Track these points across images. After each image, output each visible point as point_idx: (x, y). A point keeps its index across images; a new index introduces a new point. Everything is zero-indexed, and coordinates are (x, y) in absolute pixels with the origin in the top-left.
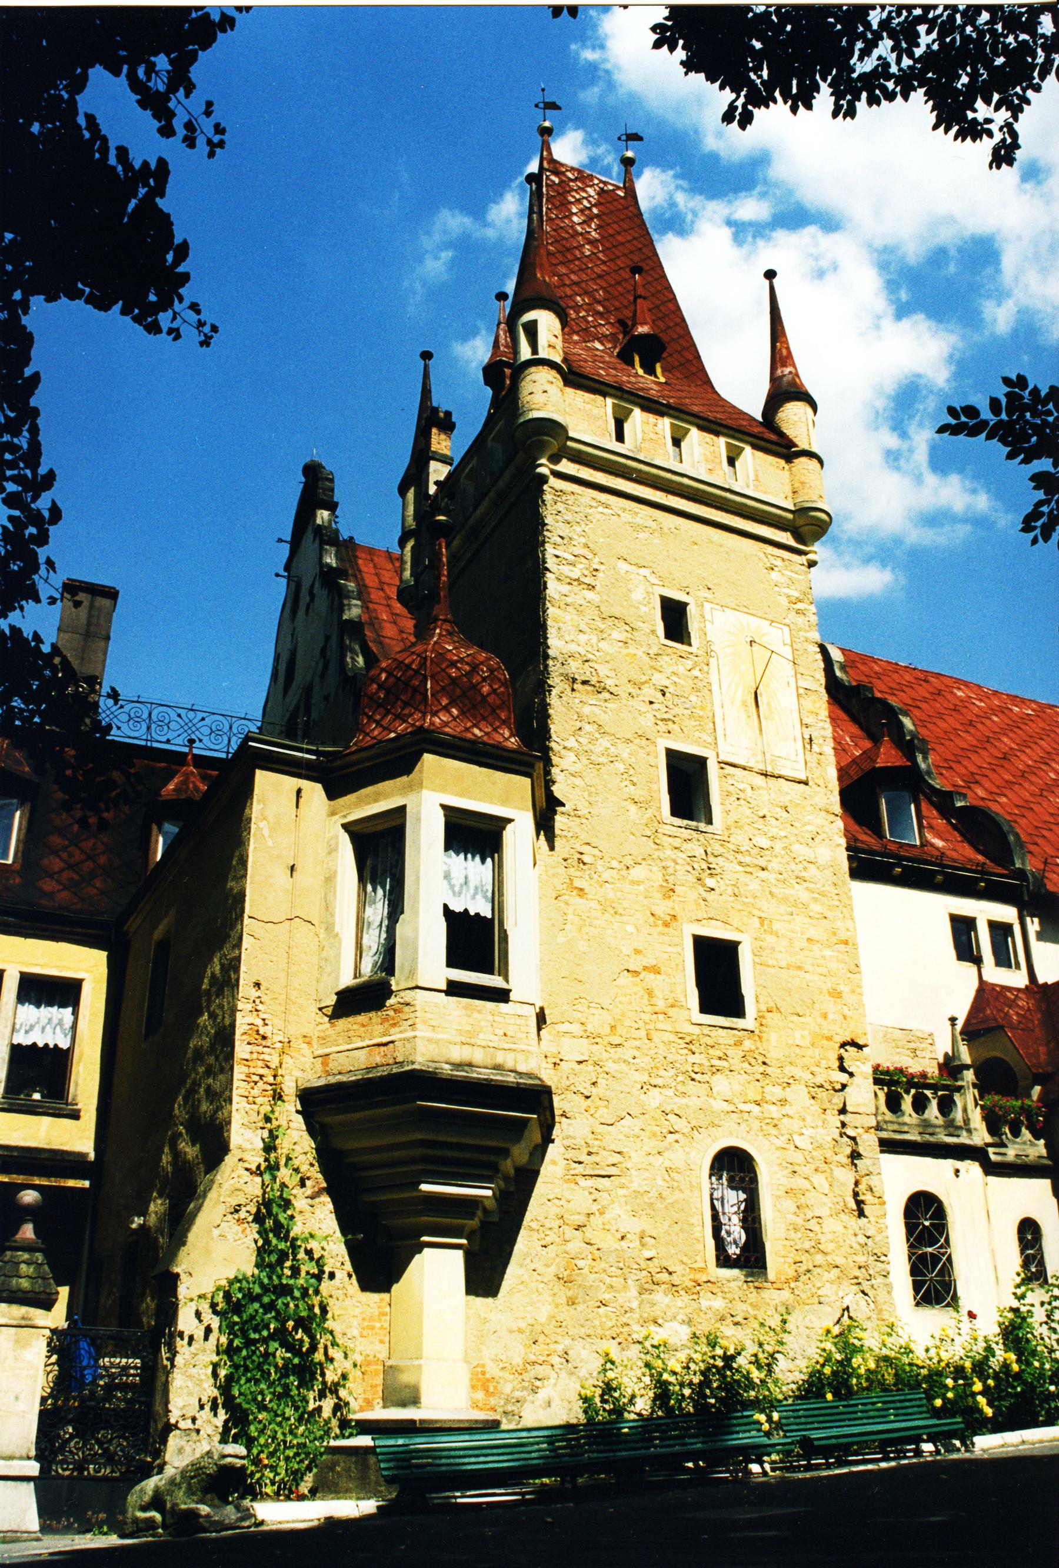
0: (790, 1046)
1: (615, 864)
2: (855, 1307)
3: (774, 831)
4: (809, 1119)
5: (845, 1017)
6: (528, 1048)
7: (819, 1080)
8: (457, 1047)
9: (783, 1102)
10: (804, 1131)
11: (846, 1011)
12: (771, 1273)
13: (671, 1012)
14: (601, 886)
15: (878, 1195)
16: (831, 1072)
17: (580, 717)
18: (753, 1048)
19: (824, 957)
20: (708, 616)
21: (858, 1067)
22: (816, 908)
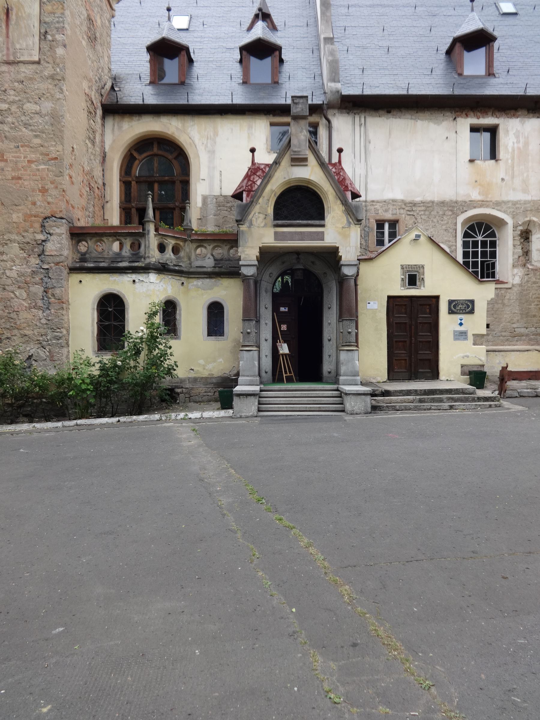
0: (8, 223)
2: (37, 355)
3: (12, 98)
4: (17, 261)
5: (49, 203)
7: (28, 240)
10: (14, 268)
11: (50, 199)
15: (57, 298)
16: (36, 235)
19: (38, 170)
21: (54, 230)
22: (37, 141)
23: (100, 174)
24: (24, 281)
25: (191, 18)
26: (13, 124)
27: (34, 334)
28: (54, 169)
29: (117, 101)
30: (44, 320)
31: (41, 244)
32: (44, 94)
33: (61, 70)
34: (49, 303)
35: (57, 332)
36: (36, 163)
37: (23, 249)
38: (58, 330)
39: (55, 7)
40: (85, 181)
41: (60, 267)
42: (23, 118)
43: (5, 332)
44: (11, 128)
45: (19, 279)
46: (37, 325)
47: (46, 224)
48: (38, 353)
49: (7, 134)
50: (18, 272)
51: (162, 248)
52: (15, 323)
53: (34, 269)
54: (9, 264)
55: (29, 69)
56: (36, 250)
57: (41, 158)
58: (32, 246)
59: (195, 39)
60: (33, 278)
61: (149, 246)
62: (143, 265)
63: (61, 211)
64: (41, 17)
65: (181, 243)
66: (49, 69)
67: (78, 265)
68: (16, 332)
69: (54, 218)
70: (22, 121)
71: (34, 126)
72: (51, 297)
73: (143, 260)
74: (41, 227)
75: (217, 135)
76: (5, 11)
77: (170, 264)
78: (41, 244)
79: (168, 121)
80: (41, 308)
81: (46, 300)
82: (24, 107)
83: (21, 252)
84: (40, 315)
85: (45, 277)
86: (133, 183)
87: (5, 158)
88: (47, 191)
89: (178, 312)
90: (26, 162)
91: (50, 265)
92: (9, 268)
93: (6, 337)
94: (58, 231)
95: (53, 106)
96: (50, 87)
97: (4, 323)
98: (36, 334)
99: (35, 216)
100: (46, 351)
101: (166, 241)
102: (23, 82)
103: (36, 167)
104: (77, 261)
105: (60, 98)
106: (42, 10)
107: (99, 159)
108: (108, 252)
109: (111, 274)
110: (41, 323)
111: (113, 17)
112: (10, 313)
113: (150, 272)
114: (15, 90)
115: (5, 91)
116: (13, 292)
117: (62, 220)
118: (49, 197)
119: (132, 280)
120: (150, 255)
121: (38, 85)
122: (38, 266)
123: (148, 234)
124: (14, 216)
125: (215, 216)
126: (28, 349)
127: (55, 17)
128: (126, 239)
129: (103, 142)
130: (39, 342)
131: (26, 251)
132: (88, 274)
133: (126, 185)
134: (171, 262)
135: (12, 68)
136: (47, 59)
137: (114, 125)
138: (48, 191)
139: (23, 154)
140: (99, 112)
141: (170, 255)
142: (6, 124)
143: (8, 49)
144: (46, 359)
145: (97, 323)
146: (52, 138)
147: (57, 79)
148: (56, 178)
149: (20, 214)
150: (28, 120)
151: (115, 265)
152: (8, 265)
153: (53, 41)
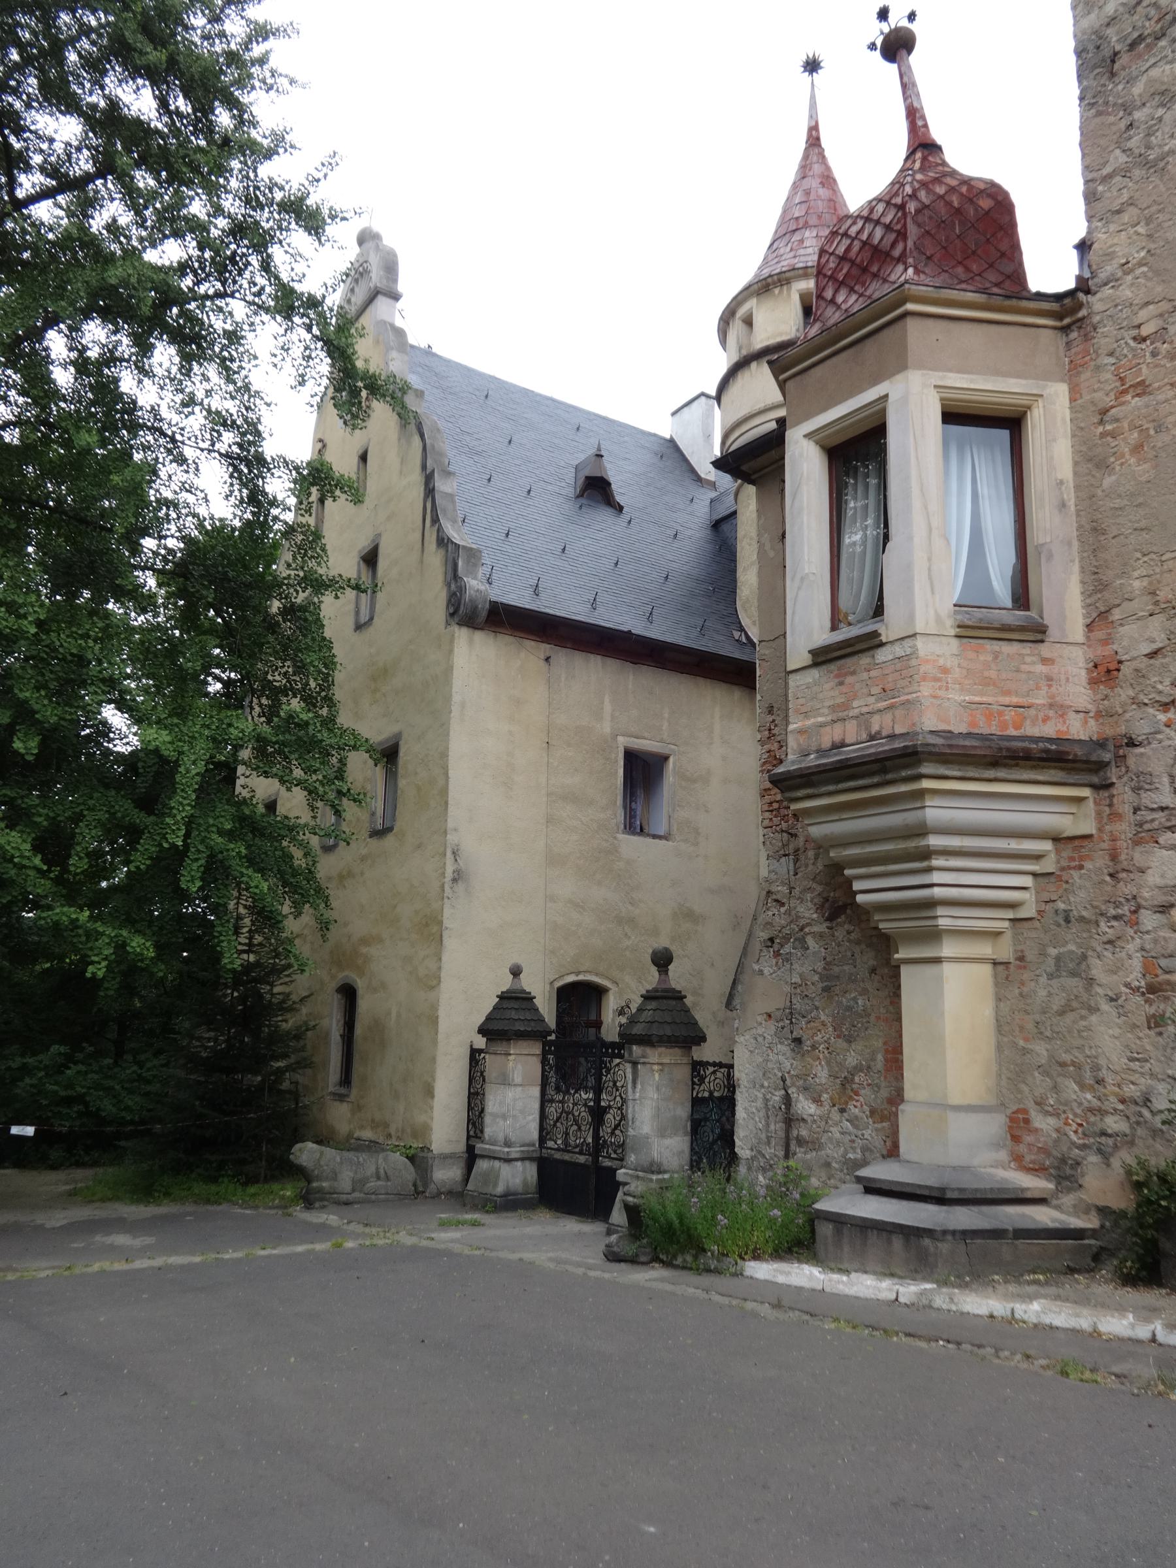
6: (909, 697)
8: (828, 729)
17: (1128, 109)
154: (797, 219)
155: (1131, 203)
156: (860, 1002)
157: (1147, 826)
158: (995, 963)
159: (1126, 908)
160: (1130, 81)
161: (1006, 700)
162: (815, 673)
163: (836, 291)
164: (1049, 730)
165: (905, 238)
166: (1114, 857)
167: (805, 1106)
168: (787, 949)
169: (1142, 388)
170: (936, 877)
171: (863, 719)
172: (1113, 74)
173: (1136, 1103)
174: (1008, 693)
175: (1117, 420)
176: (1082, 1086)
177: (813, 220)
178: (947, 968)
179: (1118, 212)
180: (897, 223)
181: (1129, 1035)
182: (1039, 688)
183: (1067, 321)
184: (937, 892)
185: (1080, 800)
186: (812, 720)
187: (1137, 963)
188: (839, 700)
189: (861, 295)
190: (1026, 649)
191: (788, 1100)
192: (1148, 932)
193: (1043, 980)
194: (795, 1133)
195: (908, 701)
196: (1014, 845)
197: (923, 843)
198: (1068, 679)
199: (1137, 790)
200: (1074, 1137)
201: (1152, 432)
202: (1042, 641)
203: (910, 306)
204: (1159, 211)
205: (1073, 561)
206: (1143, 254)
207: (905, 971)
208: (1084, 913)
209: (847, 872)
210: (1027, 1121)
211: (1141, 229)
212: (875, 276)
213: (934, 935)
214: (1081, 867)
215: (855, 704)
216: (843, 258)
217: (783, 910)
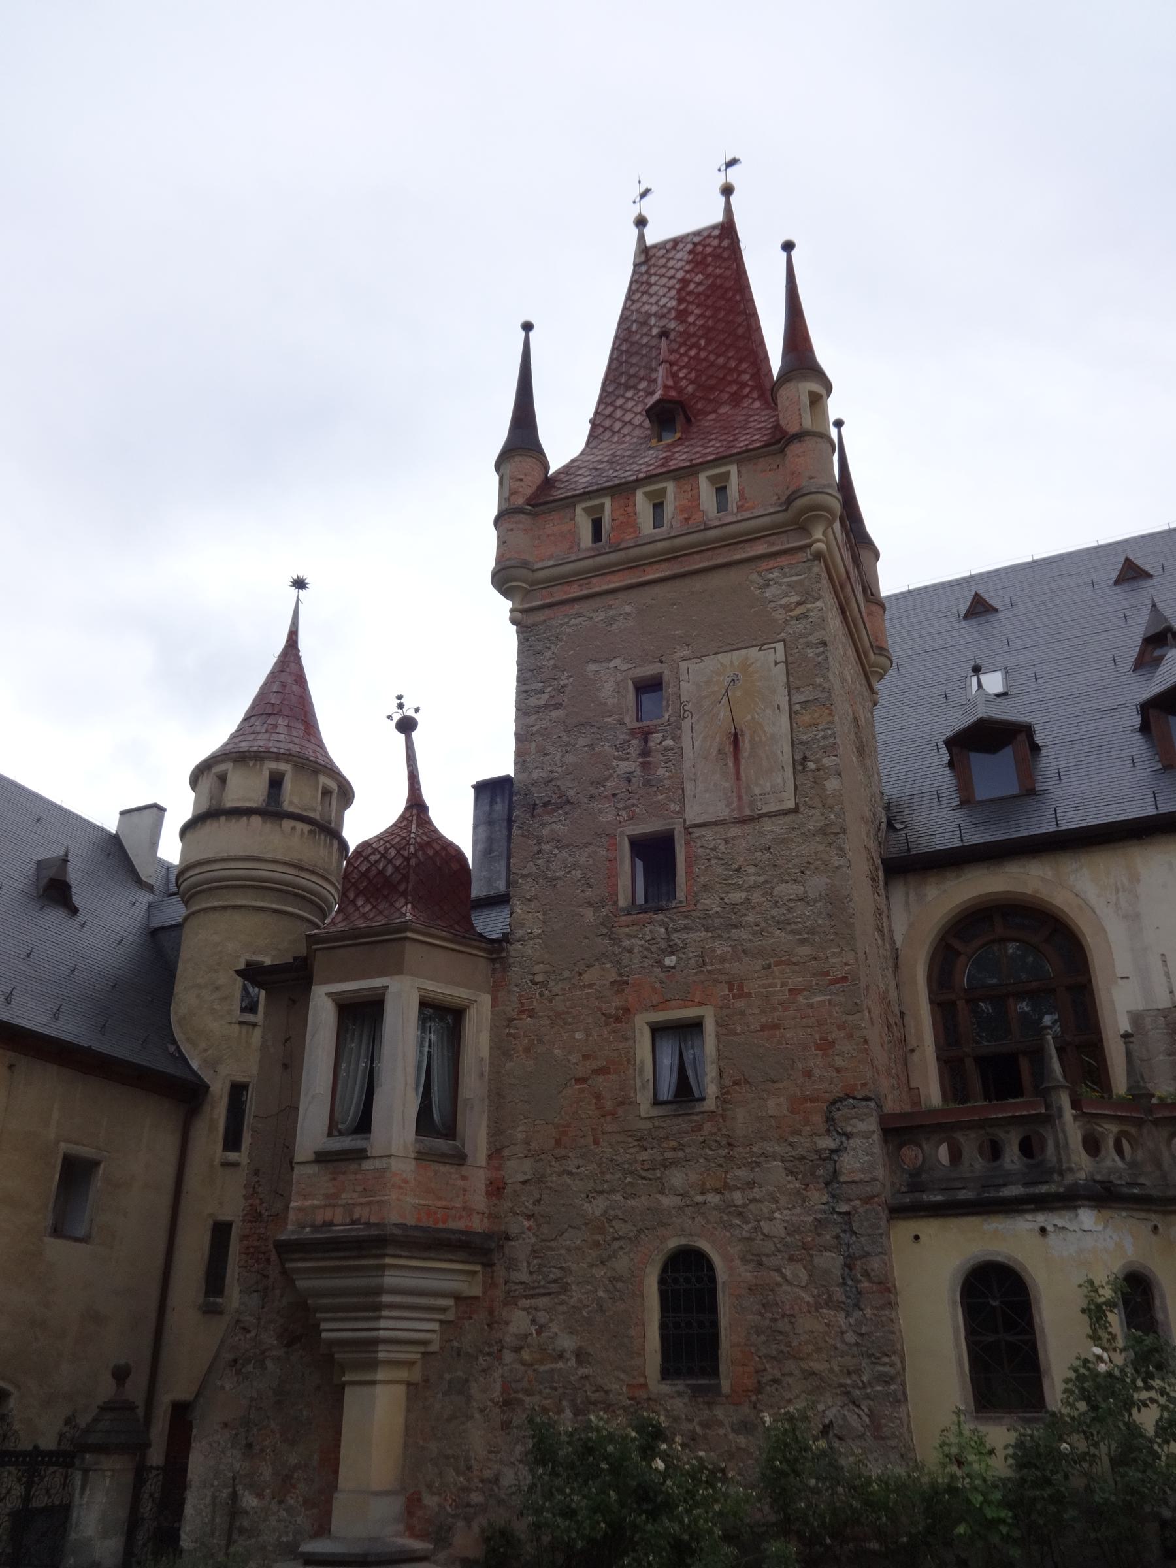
1: (567, 974)
2: (841, 1422)
3: (751, 880)
4: (783, 1200)
6: (383, 1198)
7: (800, 1151)
9: (751, 1185)
10: (777, 1215)
11: (839, 1062)
12: (726, 1386)
13: (620, 1111)
14: (551, 1001)
16: (816, 1139)
17: (540, 841)
18: (714, 1130)
19: (811, 1006)
20: (684, 676)
22: (805, 950)
23: (896, 994)
24: (800, 1244)
25: (1007, 672)
26: (758, 926)
27: (831, 1371)
28: (842, 999)
29: (909, 850)
30: (852, 1333)
31: (829, 1158)
32: (809, 863)
33: (837, 816)
34: (860, 1293)
35: (884, 1364)
36: (805, 993)
37: (792, 1173)
38: (886, 1360)
39: (816, 715)
40: (883, 1015)
41: (875, 1206)
42: (775, 912)
43: (768, 1367)
44: (754, 934)
45: (788, 1239)
46: (836, 1349)
47: (837, 1115)
48: (844, 1418)
49: (748, 945)
50: (786, 1225)
51: (1092, 1145)
52: (789, 1345)
53: (819, 1216)
54: (766, 1207)
55: (779, 824)
56: (820, 1172)
57: (814, 982)
58: (811, 1163)
59: (1029, 708)
60: (819, 1235)
61: (1067, 1144)
62: (1061, 1190)
63: (865, 1085)
64: (794, 735)
65: (1133, 1131)
66: (815, 818)
67: (908, 1200)
68: (790, 1365)
69: (851, 1100)
70: (773, 917)
71: (795, 923)
72: (860, 1277)
73: (1056, 1177)
74: (827, 1122)
75: (1138, 881)
76: (732, 739)
77: (1119, 1182)
78: (829, 1158)
79: (1022, 870)
80: (843, 1306)
81: (851, 1287)
82: (775, 892)
83: (790, 1178)
84: (843, 1325)
85: (845, 1231)
86: (961, 1004)
87: (746, 990)
88: (832, 1044)
89: (1157, 1303)
90: (787, 993)
91: (852, 1203)
92: (767, 1215)
93: (770, 1377)
94: (862, 1126)
95: (829, 881)
96: (821, 848)
97: (764, 1343)
98: (837, 1369)
99: (812, 1100)
100: (861, 1413)
101: (1100, 1129)
102: (770, 848)
103: (805, 1001)
104: (903, 1189)
105: (840, 866)
106: (795, 725)
107: (890, 963)
108: (971, 1165)
109: (985, 1217)
110: (843, 1342)
111: (875, 704)
112: (776, 1320)
113: (1079, 1207)
114: (756, 866)
115: (739, 869)
116: (778, 1270)
117: (869, 1103)
118: (837, 1057)
119: (1037, 1227)
120: (1073, 1165)
121: (797, 849)
122: (827, 1207)
123: (1060, 1116)
124: (771, 1103)
125: (1169, 1055)
126: (821, 1407)
127: (817, 731)
128: (1008, 1132)
129: (891, 930)
130: (843, 1389)
131: (800, 1176)
132: (931, 1220)
133: (943, 1009)
134: (1120, 1178)
135: (748, 829)
136: (810, 803)
137: (907, 894)
138: (834, 1046)
139: (779, 978)
140: (881, 874)
141: (1113, 1160)
142: (744, 927)
143: (740, 798)
144: (864, 1434)
145: (965, 1338)
146: (832, 940)
147: (832, 833)
148: (850, 1018)
149: (782, 1099)
150: (784, 914)
151: (992, 1194)
152: (765, 1210)
153: (818, 770)
154: (273, 704)
155: (535, 897)
156: (305, 1413)
157: (511, 1294)
158: (409, 1384)
159: (495, 1348)
160: (543, 825)
161: (440, 1204)
162: (315, 1168)
163: (357, 896)
164: (460, 1225)
165: (408, 882)
166: (491, 1313)
167: (250, 1501)
168: (250, 1368)
169: (532, 1013)
170: (382, 1324)
171: (350, 1208)
172: (533, 816)
173: (490, 1482)
174: (440, 1199)
175: (517, 1028)
176: (458, 1473)
177: (286, 711)
178: (379, 1389)
179: (528, 900)
180: (404, 868)
181: (490, 1435)
182: (458, 1196)
183: (494, 956)
184: (382, 1333)
185: (475, 1273)
186: (310, 1202)
187: (498, 1386)
188: (332, 1191)
189: (374, 907)
190: (453, 1169)
191: (234, 1496)
192: (507, 1365)
193: (440, 1395)
194: (237, 1524)
195: (382, 1201)
196: (432, 1301)
197: (379, 1299)
198: (475, 1190)
199: (508, 1269)
200: (448, 1508)
201: (536, 1042)
202: (463, 1165)
203: (409, 934)
204: (550, 910)
205: (484, 1112)
206: (540, 931)
207: (348, 1391)
208: (470, 1350)
209: (318, 1315)
210: (419, 1500)
211: (540, 915)
212: (385, 897)
213: (374, 1365)
214: (470, 1318)
215: (343, 1196)
216: (364, 875)
217: (248, 1336)
